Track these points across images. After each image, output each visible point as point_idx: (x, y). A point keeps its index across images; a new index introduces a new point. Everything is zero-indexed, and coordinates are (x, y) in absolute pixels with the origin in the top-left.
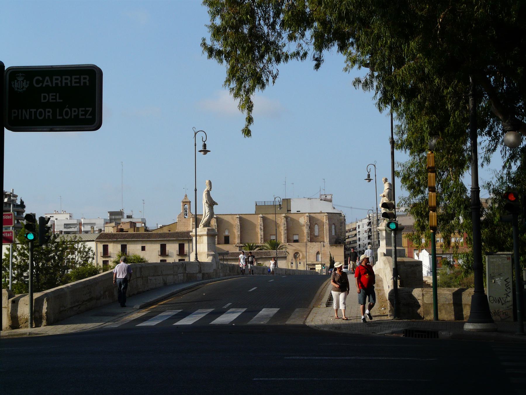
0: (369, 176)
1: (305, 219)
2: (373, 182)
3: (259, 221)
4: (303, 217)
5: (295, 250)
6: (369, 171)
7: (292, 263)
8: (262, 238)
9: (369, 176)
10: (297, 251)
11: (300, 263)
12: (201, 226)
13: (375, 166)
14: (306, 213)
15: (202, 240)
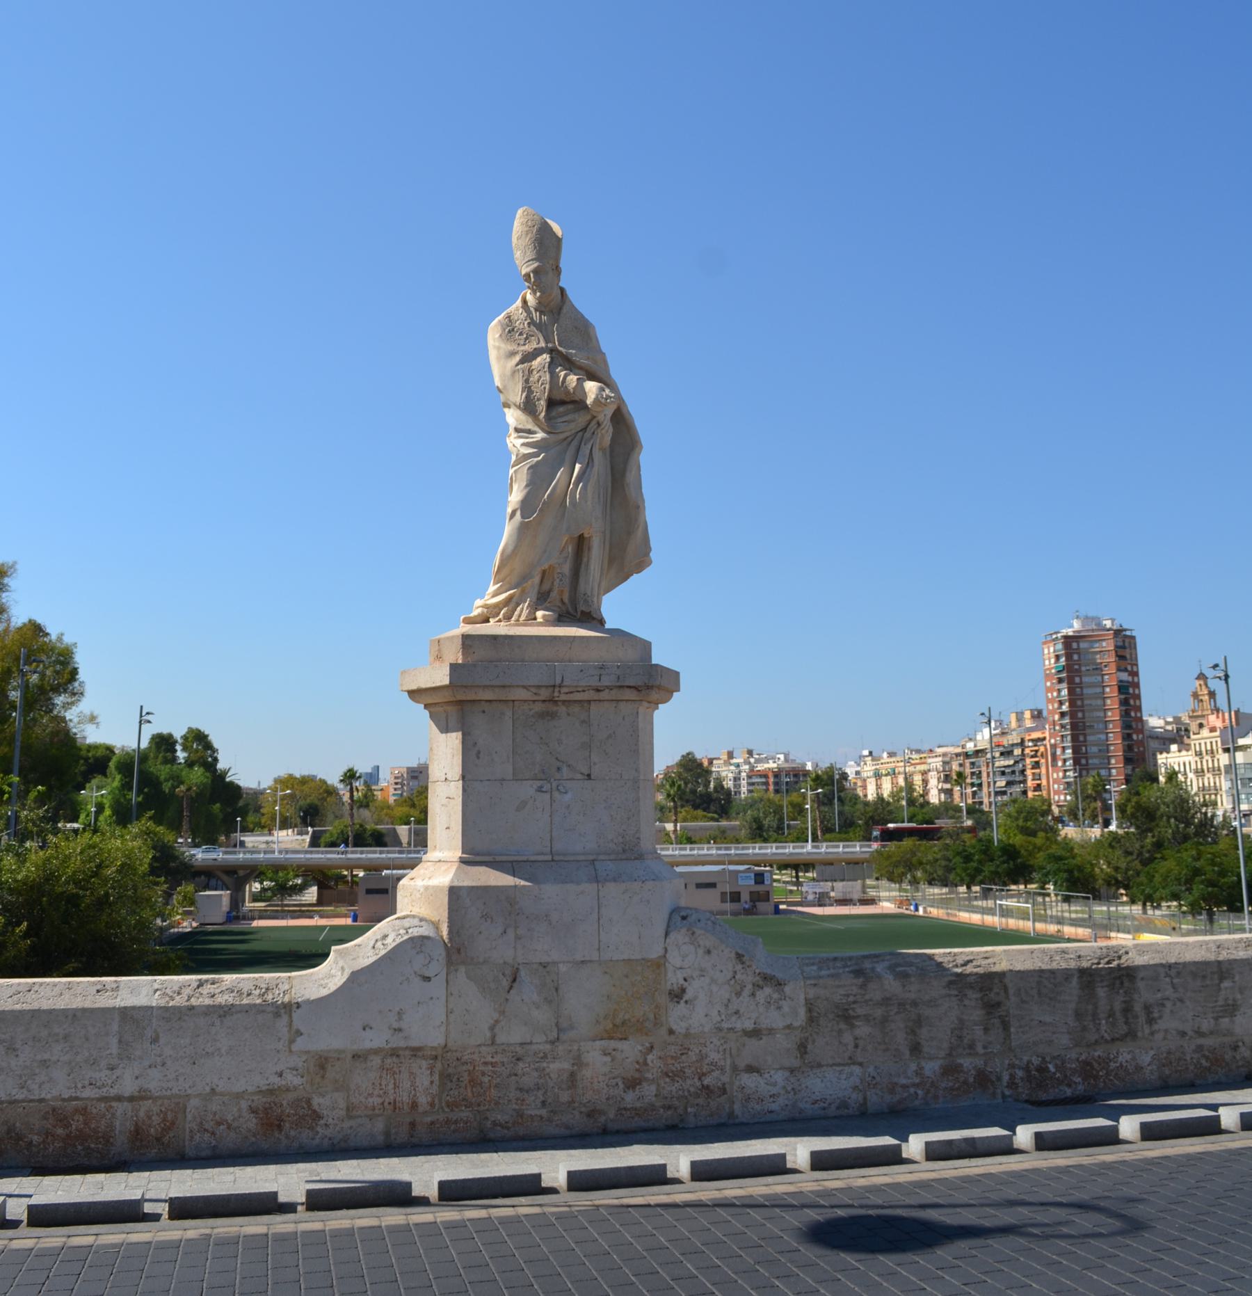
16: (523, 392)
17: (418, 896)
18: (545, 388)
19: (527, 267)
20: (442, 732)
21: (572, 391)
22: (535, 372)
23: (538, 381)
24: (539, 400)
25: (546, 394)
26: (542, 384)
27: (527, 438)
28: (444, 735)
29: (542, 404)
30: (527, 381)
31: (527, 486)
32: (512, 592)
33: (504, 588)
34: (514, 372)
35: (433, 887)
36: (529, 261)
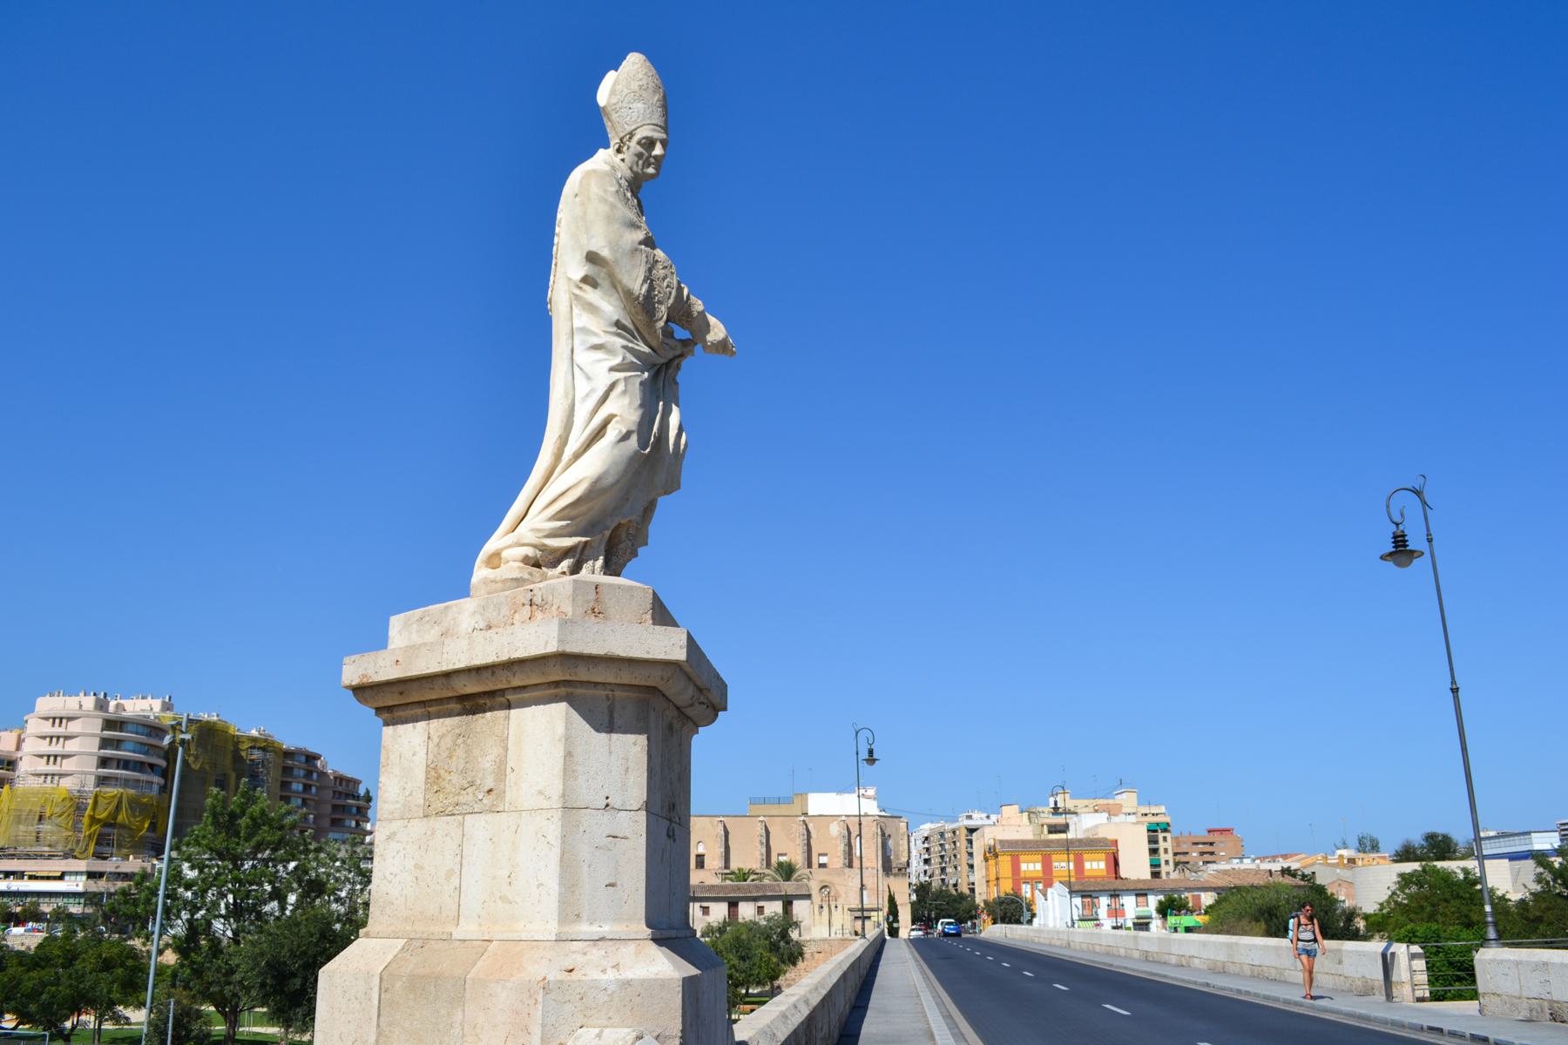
0: (1400, 541)
1: (839, 826)
2: (1420, 565)
3: (759, 829)
4: (835, 823)
5: (823, 881)
6: (1397, 519)
7: (822, 907)
8: (763, 860)
9: (1400, 541)
10: (825, 884)
11: (836, 907)
12: (495, 560)
13: (1418, 493)
14: (839, 816)
15: (487, 763)
16: (644, 281)
17: (603, 998)
18: (670, 293)
19: (654, 130)
20: (598, 729)
21: (695, 314)
22: (660, 266)
23: (664, 279)
24: (660, 302)
25: (671, 301)
26: (668, 286)
27: (632, 342)
28: (604, 735)
29: (662, 311)
30: (650, 270)
31: (642, 406)
32: (576, 540)
33: (569, 529)
34: (636, 250)
35: (643, 982)
36: (657, 125)
